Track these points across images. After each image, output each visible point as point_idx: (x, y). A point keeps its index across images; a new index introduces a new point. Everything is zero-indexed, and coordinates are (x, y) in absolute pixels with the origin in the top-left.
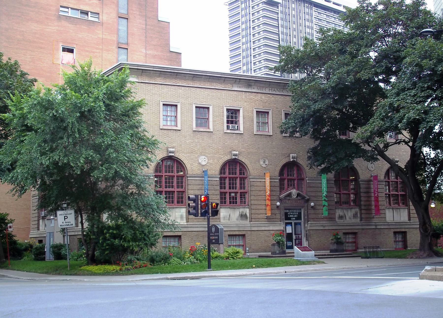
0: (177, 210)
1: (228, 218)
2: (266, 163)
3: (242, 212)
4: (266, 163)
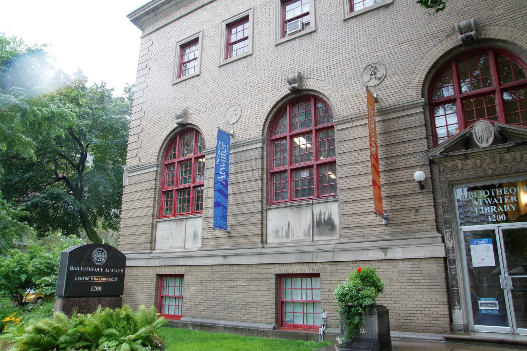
0: (189, 222)
1: (284, 234)
2: (379, 75)
3: (320, 214)
4: (379, 75)
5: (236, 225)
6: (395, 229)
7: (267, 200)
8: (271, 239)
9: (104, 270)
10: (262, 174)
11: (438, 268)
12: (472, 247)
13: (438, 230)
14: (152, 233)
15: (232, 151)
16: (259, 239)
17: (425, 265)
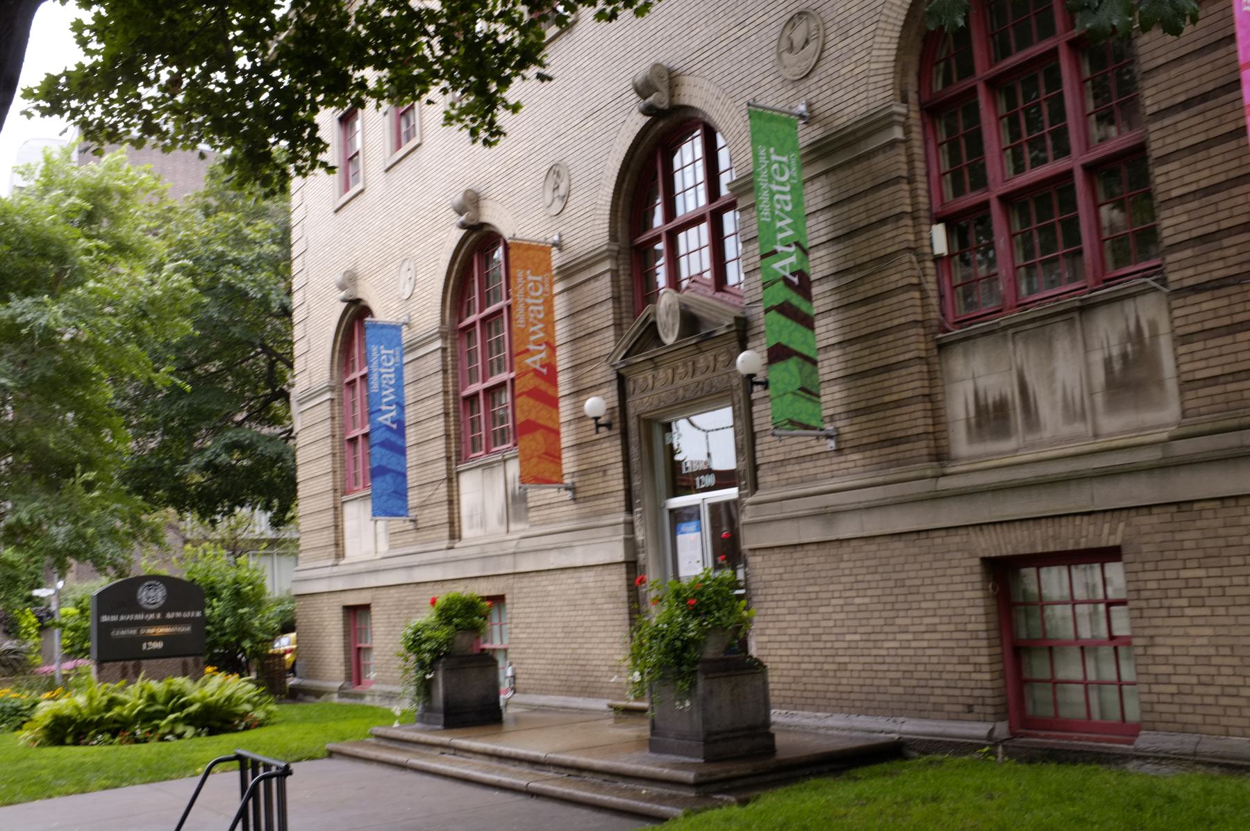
5: (422, 506)
6: (587, 508)
7: (458, 453)
8: (466, 533)
9: (164, 615)
10: (446, 403)
11: (617, 581)
12: (680, 538)
13: (629, 509)
14: (336, 526)
15: (406, 359)
16: (445, 532)
17: (607, 578)
